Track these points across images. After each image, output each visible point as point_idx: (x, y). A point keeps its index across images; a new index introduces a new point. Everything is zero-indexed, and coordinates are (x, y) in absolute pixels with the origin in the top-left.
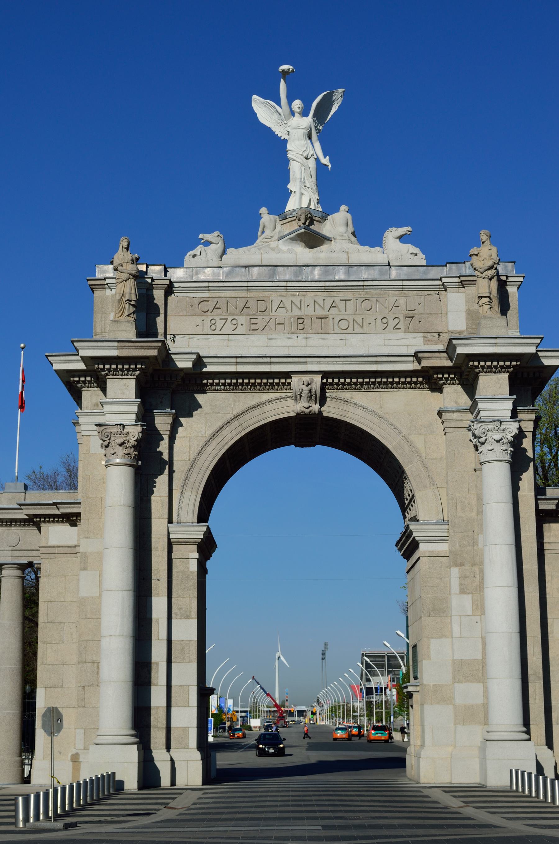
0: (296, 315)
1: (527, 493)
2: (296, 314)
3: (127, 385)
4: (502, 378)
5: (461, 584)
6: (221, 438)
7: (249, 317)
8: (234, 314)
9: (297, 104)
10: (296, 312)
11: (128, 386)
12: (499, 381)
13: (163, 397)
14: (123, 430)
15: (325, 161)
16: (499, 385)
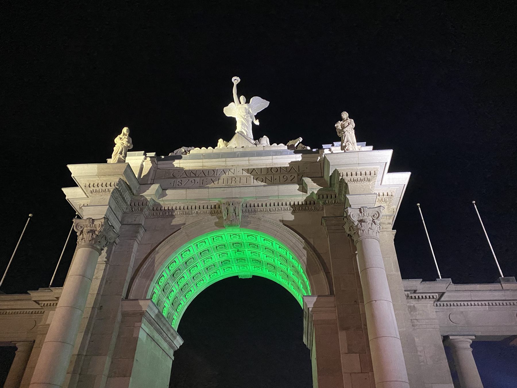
0: (231, 176)
1: (395, 273)
2: (231, 176)
3: (104, 198)
4: (365, 185)
5: (348, 345)
6: (172, 243)
7: (202, 179)
8: (193, 177)
9: (242, 98)
10: (231, 174)
11: (104, 199)
12: (363, 187)
13: (136, 217)
14: (93, 223)
15: (257, 123)
16: (363, 189)
